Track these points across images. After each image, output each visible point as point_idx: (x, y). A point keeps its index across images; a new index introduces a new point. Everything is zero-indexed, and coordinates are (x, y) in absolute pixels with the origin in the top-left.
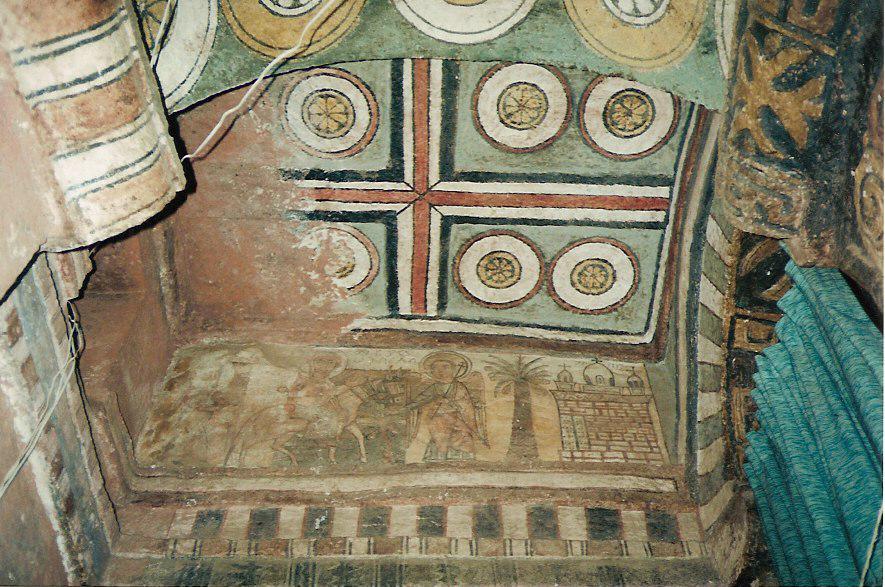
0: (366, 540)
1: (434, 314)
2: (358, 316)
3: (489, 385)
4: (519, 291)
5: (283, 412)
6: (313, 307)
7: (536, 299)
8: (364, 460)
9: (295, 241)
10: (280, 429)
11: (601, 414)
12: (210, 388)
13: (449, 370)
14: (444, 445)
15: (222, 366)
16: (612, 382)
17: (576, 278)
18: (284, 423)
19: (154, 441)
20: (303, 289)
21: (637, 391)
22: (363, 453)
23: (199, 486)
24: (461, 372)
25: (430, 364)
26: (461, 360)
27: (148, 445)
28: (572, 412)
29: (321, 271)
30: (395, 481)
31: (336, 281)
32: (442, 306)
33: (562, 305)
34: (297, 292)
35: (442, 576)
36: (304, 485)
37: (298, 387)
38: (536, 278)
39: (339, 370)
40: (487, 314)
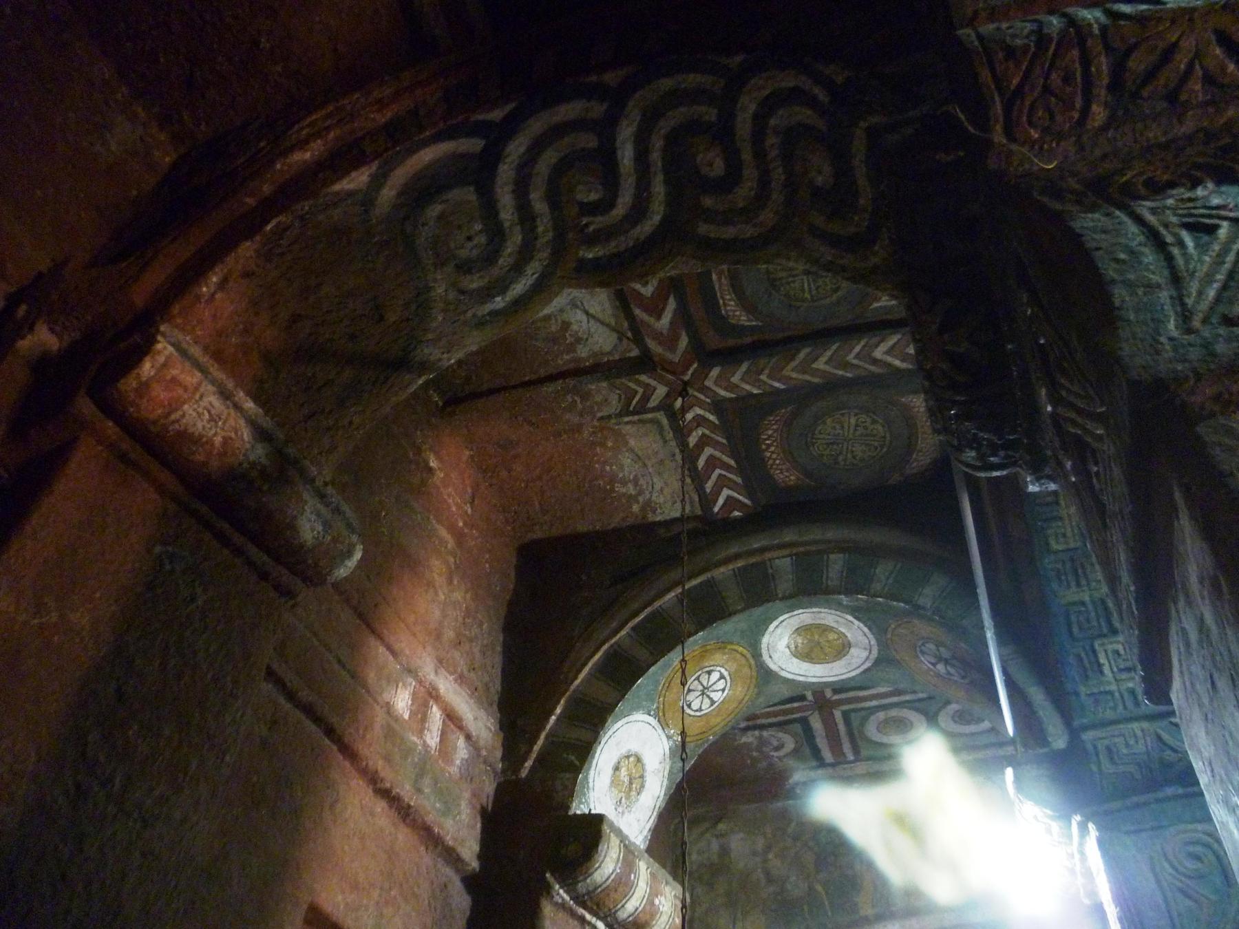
5: (762, 876)
29: (761, 752)
31: (772, 753)
32: (856, 750)
37: (768, 848)
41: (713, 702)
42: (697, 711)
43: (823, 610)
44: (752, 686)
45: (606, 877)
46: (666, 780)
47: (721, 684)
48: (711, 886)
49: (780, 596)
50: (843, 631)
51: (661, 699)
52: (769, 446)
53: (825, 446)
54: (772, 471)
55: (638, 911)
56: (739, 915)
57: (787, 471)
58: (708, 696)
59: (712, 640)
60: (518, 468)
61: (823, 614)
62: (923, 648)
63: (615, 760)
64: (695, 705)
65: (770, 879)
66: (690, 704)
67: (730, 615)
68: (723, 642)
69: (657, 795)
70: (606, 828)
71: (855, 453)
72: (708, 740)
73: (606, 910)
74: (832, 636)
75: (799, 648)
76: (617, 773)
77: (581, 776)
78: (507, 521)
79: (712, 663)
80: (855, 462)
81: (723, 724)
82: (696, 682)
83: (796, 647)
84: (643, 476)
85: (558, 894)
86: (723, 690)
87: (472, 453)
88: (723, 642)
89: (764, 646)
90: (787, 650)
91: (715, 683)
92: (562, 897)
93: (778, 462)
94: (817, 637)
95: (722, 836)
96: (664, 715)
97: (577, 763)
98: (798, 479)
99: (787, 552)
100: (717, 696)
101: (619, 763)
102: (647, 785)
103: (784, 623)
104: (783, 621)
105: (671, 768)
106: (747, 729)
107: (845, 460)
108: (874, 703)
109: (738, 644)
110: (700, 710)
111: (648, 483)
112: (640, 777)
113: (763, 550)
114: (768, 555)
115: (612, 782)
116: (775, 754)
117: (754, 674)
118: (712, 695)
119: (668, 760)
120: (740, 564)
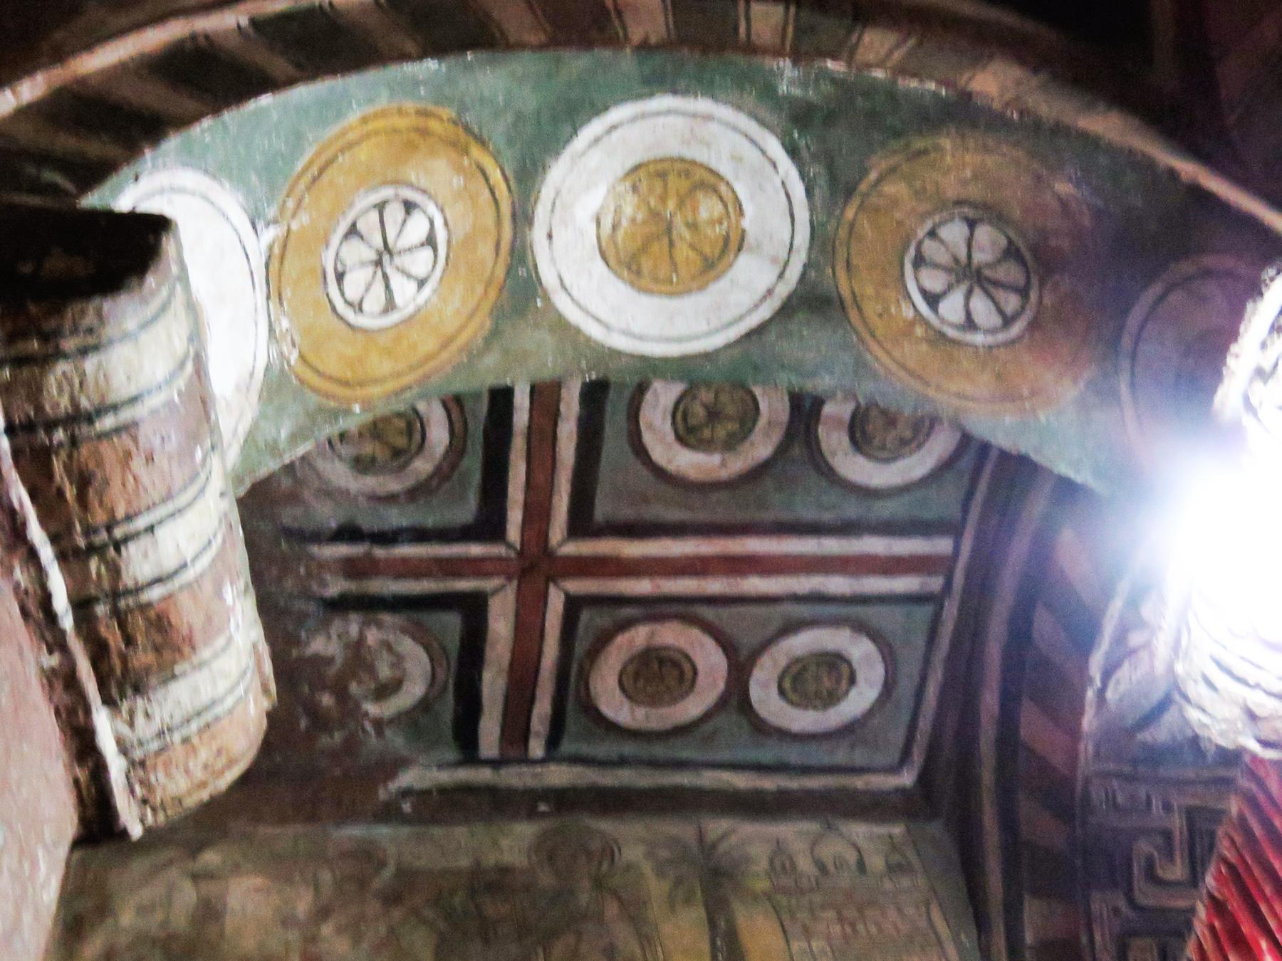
3: (656, 888)
4: (692, 707)
7: (720, 721)
11: (855, 930)
16: (861, 865)
17: (787, 684)
21: (905, 882)
25: (548, 850)
28: (807, 934)
29: (342, 694)
32: (553, 741)
33: (761, 729)
37: (323, 913)
38: (721, 685)
40: (629, 749)
41: (390, 306)
44: (486, 306)
58: (385, 277)
61: (713, 127)
74: (708, 208)
75: (620, 234)
79: (423, 183)
82: (374, 215)
83: (615, 227)
89: (546, 192)
94: (671, 204)
100: (404, 291)
103: (615, 135)
104: (613, 128)
106: (340, 605)
108: (642, 586)
109: (496, 156)
116: (372, 709)
117: (500, 272)
118: (397, 281)
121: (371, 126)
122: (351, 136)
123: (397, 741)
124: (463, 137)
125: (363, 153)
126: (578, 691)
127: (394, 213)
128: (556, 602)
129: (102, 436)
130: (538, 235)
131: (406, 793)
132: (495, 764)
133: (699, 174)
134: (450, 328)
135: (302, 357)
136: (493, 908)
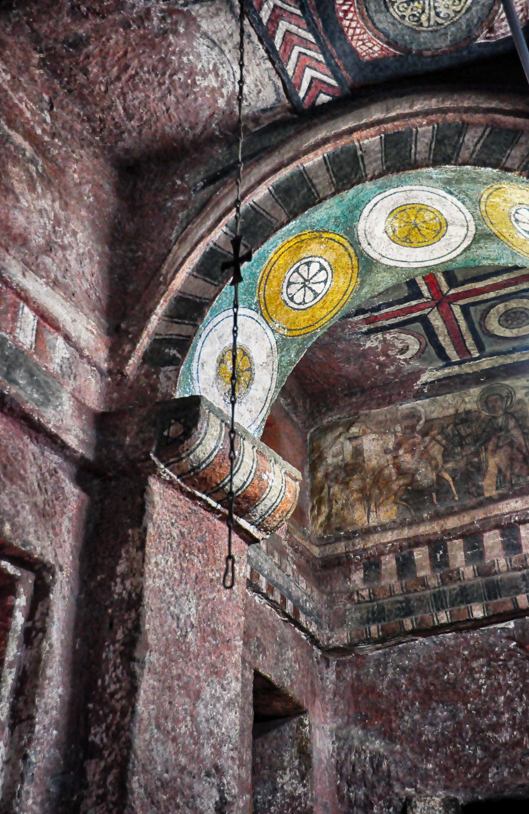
0: (471, 568)
1: (477, 355)
2: (422, 371)
6: (389, 374)
8: (457, 498)
9: (360, 346)
10: (395, 487)
12: (340, 463)
13: (499, 403)
14: (508, 474)
15: (342, 444)
18: (396, 480)
19: (319, 514)
20: (377, 367)
22: (455, 492)
23: (359, 544)
24: (509, 403)
26: (506, 391)
27: (315, 518)
29: (388, 356)
30: (480, 514)
31: (398, 357)
34: (374, 369)
35: (524, 583)
36: (423, 529)
37: (398, 445)
39: (422, 422)
41: (316, 295)
42: (300, 304)
43: (414, 188)
44: (355, 275)
45: (209, 452)
46: (275, 373)
47: (322, 276)
48: (346, 484)
49: (369, 176)
50: (438, 208)
51: (261, 293)
52: (346, 12)
53: (405, 5)
54: (354, 43)
55: (246, 485)
56: (373, 508)
57: (370, 41)
58: (310, 288)
59: (307, 228)
60: (94, 70)
61: (415, 192)
62: (516, 215)
63: (219, 353)
64: (298, 298)
65: (401, 472)
66: (293, 297)
67: (320, 202)
68: (317, 231)
69: (267, 387)
70: (204, 408)
71: (438, 10)
72: (316, 333)
73: (214, 485)
75: (397, 233)
76: (223, 365)
77: (182, 367)
78: (94, 132)
80: (440, 21)
81: (329, 317)
82: (296, 274)
83: (394, 232)
84: (222, 64)
85: (164, 472)
86: (325, 282)
87: (42, 55)
88: (317, 231)
89: (361, 233)
90: (385, 234)
91: (315, 275)
92: (168, 475)
93: (358, 31)
95: (356, 438)
96: (266, 309)
97: (178, 355)
98: (382, 49)
99: (372, 130)
100: (319, 288)
101: (223, 356)
102: (256, 377)
103: (377, 206)
104: (376, 204)
105: (280, 361)
107: (429, 20)
108: (492, 295)
109: (334, 232)
110: (304, 302)
111: (228, 72)
112: (247, 370)
113: (351, 131)
114: (355, 135)
115: (218, 374)
116: (402, 357)
117: (355, 262)
118: (314, 287)
119: (276, 354)
120: (329, 148)
121: (280, 252)
122: (273, 260)
123: (416, 364)
124: (317, 234)
125: (281, 261)
126: (483, 332)
127: (303, 270)
128: (457, 310)
129: (203, 469)
130: (364, 245)
131: (424, 384)
132: (459, 363)
133: (418, 207)
134: (345, 289)
135: (289, 330)
136: (464, 430)
